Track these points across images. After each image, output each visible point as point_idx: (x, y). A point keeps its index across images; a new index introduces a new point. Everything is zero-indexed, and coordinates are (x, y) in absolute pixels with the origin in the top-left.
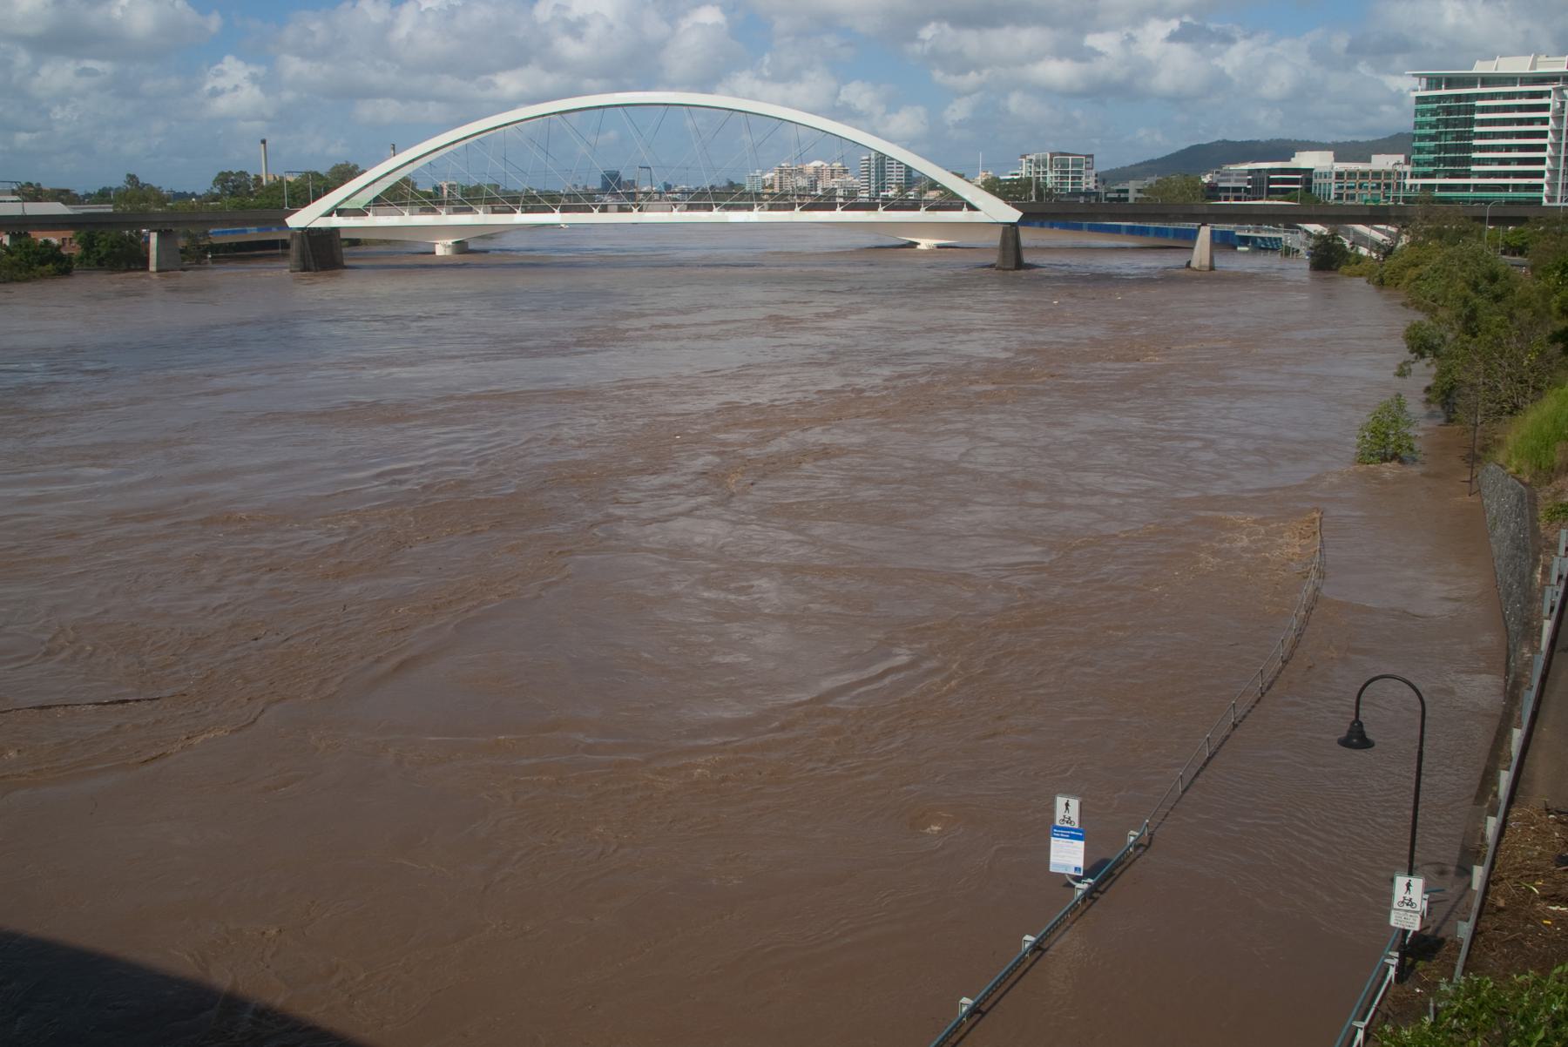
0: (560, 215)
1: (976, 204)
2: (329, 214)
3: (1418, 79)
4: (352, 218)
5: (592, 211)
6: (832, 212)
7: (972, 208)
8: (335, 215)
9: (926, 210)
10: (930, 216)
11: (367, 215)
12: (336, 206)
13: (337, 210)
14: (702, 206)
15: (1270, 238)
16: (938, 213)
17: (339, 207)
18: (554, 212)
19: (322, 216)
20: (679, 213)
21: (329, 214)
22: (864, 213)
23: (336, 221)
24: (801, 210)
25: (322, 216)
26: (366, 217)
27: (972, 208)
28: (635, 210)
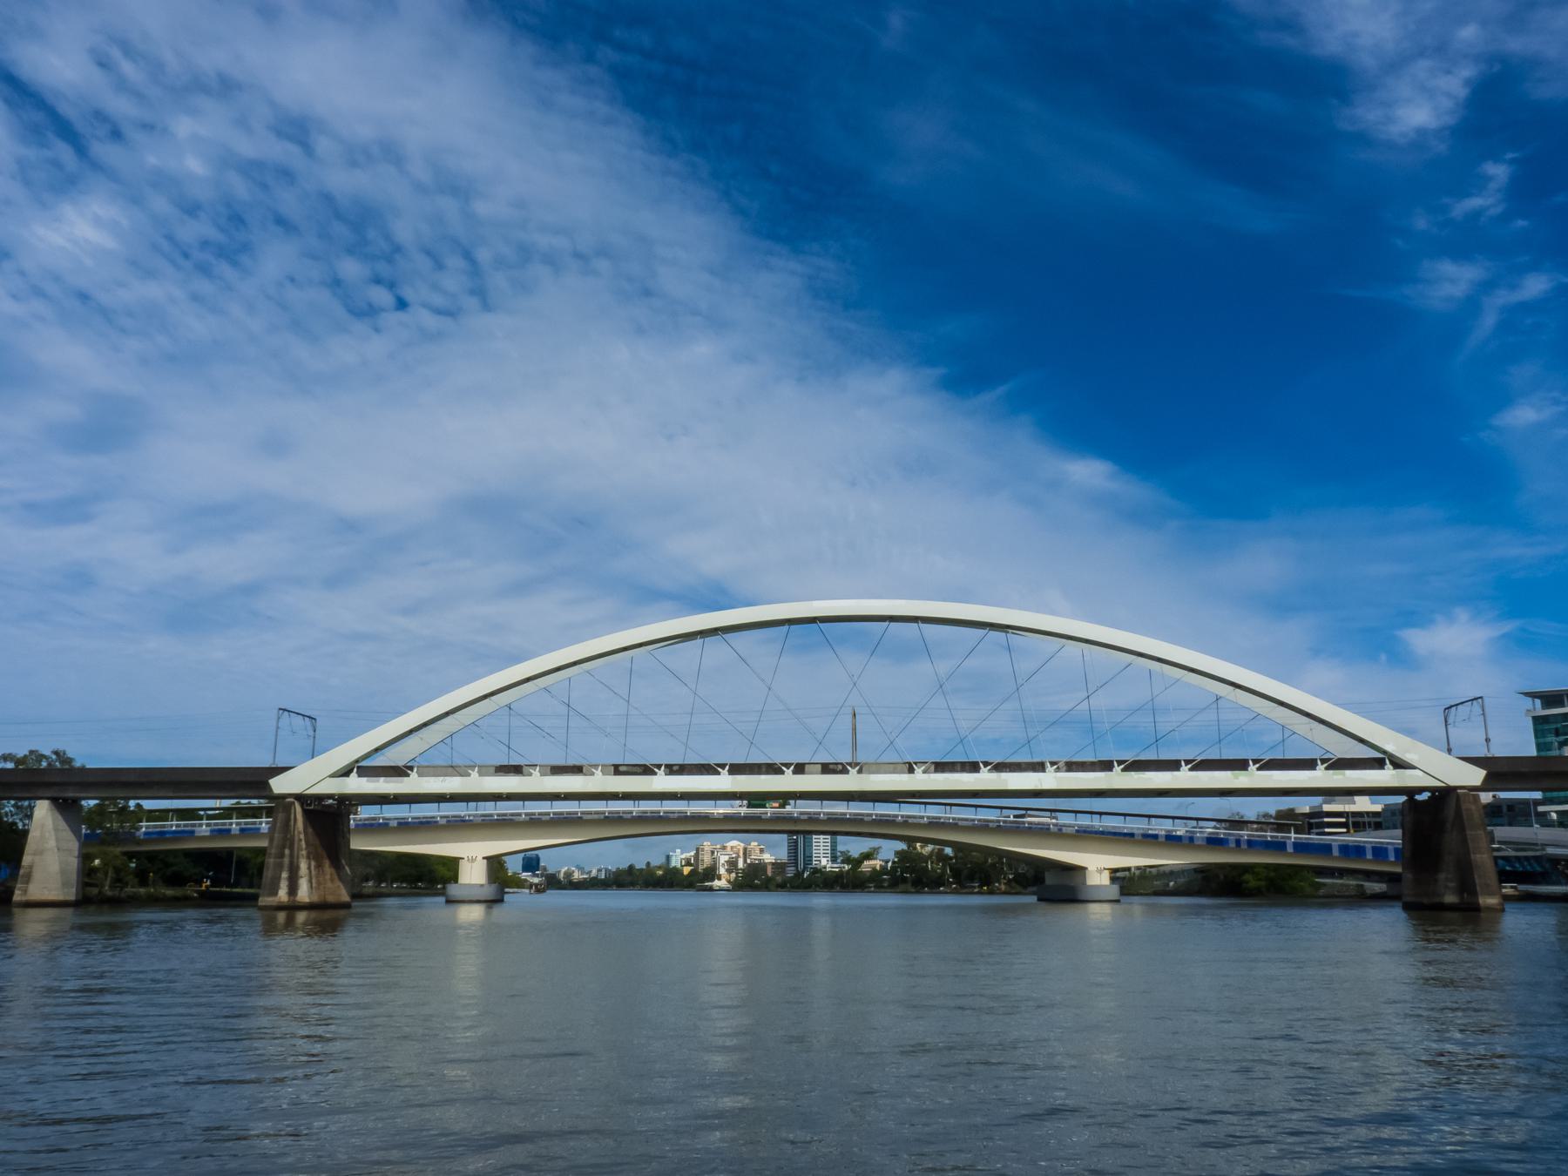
0: (731, 777)
1: (1409, 757)
2: (345, 773)
3: (1530, 699)
4: (382, 779)
5: (782, 773)
6: (1176, 773)
7: (1399, 764)
8: (354, 774)
9: (1327, 769)
10: (1335, 777)
11: (408, 775)
12: (357, 761)
13: (358, 767)
14: (959, 767)
15: (1517, 857)
16: (1349, 773)
17: (363, 764)
18: (719, 773)
19: (333, 776)
20: (926, 775)
21: (345, 773)
22: (1229, 773)
23: (356, 785)
24: (1123, 770)
25: (333, 776)
26: (405, 778)
27: (1399, 764)
28: (853, 771)
